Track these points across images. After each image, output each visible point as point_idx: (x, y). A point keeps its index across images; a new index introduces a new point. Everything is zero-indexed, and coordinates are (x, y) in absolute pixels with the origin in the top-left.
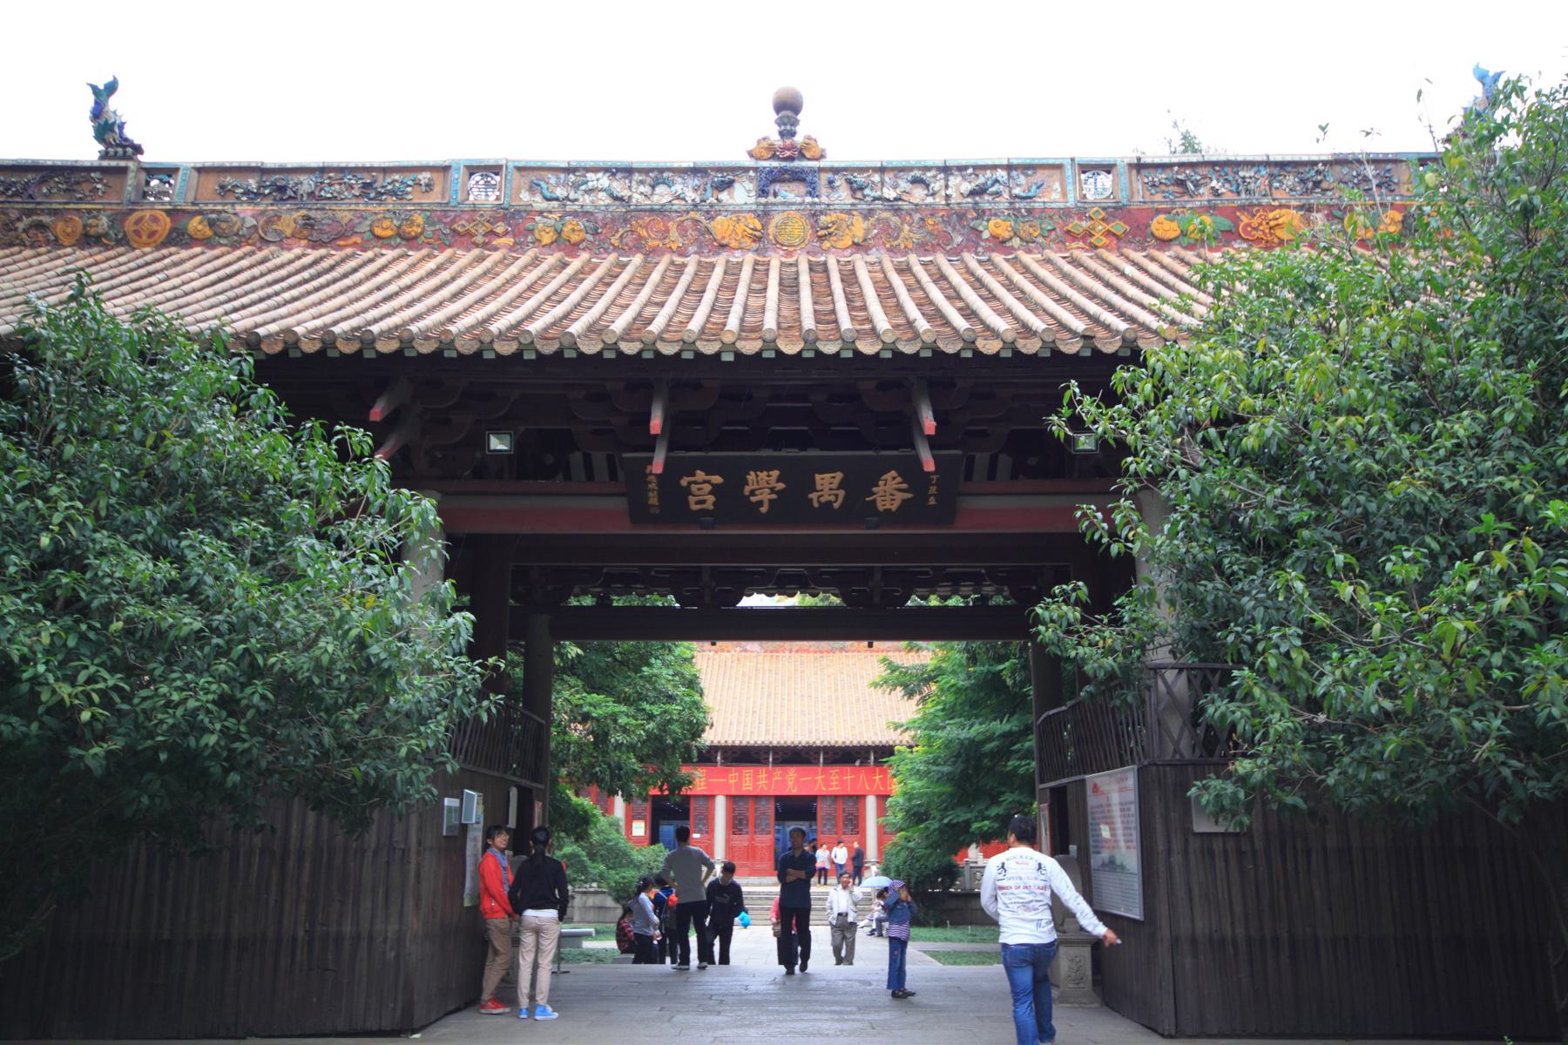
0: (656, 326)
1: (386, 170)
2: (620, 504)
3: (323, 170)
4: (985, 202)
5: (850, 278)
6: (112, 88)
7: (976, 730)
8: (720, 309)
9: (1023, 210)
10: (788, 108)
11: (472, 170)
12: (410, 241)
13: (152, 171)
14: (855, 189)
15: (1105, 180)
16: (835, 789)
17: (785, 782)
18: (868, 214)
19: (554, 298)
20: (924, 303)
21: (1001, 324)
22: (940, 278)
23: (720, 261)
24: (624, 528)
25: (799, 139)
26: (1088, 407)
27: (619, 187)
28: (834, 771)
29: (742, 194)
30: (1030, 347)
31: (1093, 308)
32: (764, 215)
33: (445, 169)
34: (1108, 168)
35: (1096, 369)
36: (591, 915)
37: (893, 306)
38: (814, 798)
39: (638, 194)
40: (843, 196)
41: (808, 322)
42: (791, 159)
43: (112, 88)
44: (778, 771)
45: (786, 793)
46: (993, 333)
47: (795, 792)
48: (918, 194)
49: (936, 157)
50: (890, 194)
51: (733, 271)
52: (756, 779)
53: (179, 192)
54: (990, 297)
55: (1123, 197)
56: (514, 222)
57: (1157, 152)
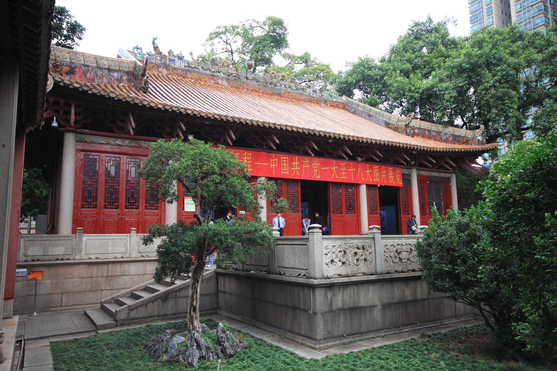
17: (311, 169)
36: (342, 324)
45: (312, 178)
47: (318, 178)
52: (291, 166)
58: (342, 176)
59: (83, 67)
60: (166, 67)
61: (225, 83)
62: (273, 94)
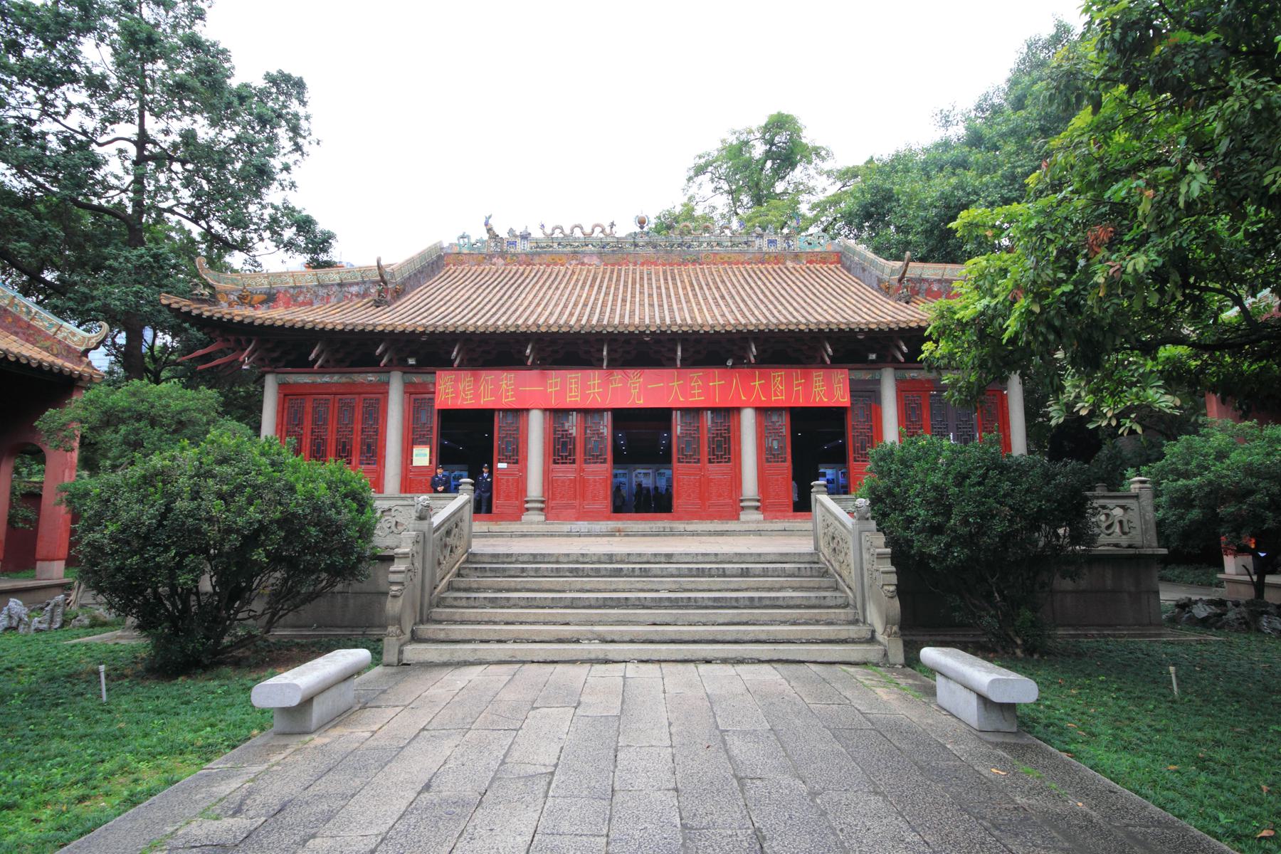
16: (697, 399)
44: (618, 375)
45: (628, 404)
47: (640, 403)
58: (693, 396)
59: (291, 291)
60: (503, 254)
61: (595, 260)
62: (684, 263)
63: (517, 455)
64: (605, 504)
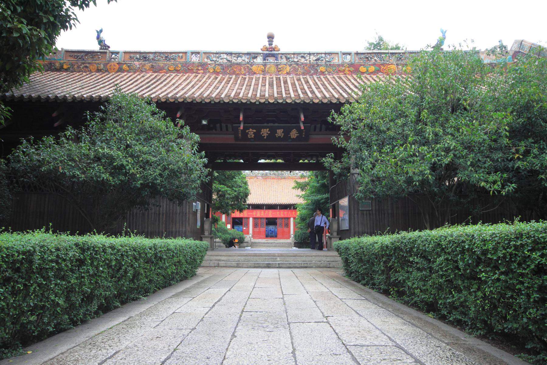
0: (241, 96)
1: (171, 53)
2: (233, 136)
3: (155, 53)
4: (319, 62)
5: (285, 82)
6: (101, 31)
7: (319, 197)
8: (255, 90)
9: (329, 65)
10: (271, 38)
11: (192, 53)
12: (178, 71)
13: (113, 53)
14: (287, 59)
15: (349, 57)
16: (282, 216)
18: (290, 65)
19: (216, 88)
20: (303, 89)
21: (319, 95)
22: (307, 82)
23: (254, 77)
24: (233, 142)
25: (273, 46)
26: (336, 116)
27: (229, 58)
28: (282, 211)
29: (259, 60)
30: (325, 101)
31: (341, 91)
32: (265, 65)
33: (186, 53)
34: (350, 54)
35: (338, 106)
37: (296, 91)
38: (276, 218)
39: (234, 60)
40: (284, 61)
41: (276, 95)
42: (271, 51)
43: (101, 31)
45: (269, 217)
46: (317, 98)
48: (303, 60)
49: (307, 51)
50: (296, 60)
51: (257, 80)
52: (261, 213)
53: (120, 58)
54: (318, 88)
55: (353, 61)
56: (203, 66)
57: (361, 50)
61: (261, 178)
62: (281, 179)
63: (248, 225)
64: (264, 236)
